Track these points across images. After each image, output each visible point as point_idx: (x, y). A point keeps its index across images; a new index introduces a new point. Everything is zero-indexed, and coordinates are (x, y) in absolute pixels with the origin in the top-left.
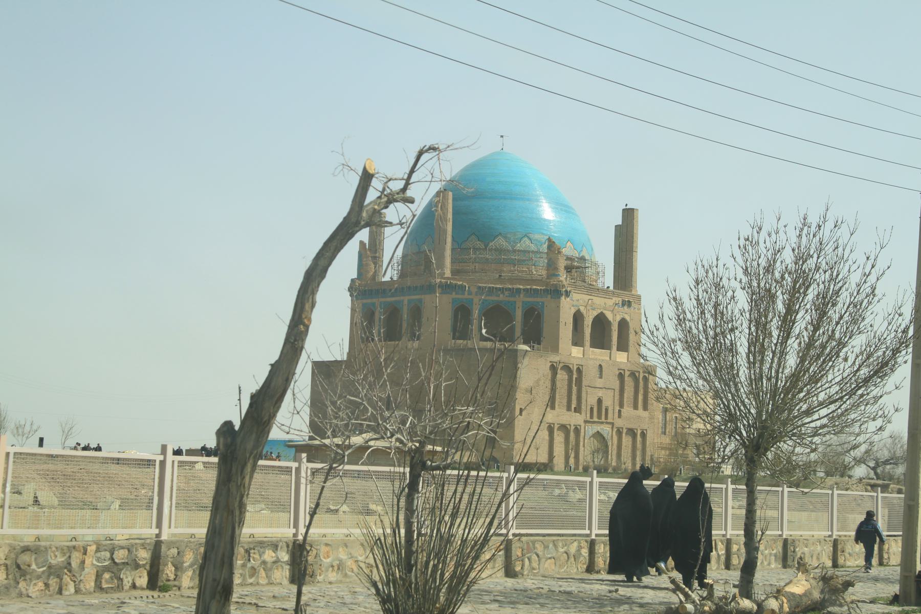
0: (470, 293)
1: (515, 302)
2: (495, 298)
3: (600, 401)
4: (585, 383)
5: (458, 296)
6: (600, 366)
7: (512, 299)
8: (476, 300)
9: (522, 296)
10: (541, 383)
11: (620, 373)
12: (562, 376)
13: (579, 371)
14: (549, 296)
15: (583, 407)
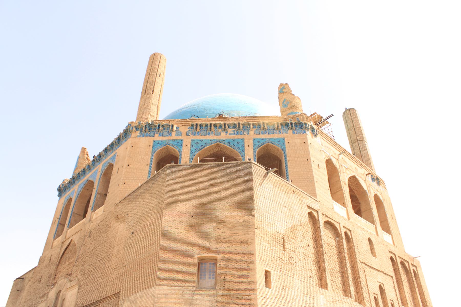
0: (179, 133)
1: (243, 140)
2: (213, 137)
3: (382, 290)
4: (359, 257)
5: (161, 138)
6: (370, 240)
7: (238, 137)
8: (187, 140)
9: (252, 132)
10: (299, 234)
11: (391, 258)
12: (327, 236)
13: (349, 239)
14: (290, 132)
15: (365, 294)
